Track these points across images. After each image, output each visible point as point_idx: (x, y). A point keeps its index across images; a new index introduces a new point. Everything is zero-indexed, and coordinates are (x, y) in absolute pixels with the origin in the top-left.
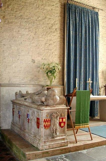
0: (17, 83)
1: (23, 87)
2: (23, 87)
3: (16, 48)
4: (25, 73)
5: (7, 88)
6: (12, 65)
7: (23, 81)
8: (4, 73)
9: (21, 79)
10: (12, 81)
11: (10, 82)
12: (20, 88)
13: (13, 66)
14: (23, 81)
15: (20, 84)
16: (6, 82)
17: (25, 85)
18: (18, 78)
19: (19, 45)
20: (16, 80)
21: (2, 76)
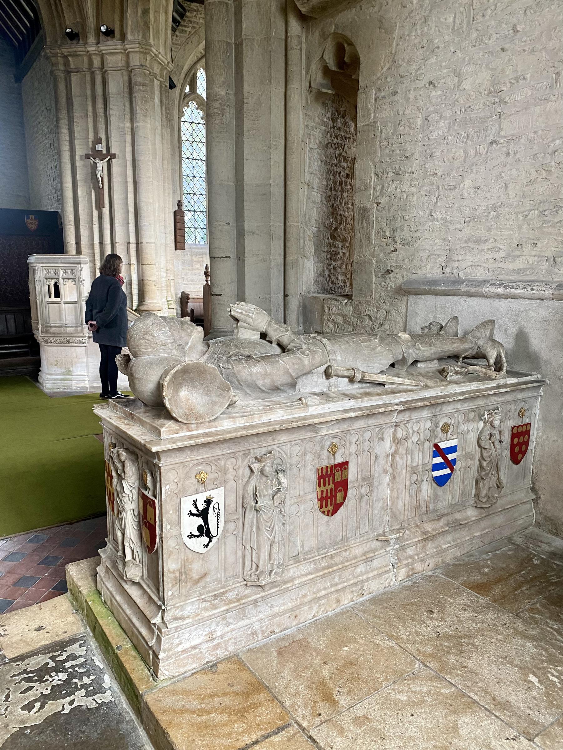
0: (480, 274)
1: (499, 296)
2: (499, 296)
3: (485, 76)
4: (526, 216)
5: (431, 300)
6: (463, 180)
7: (510, 266)
8: (426, 227)
9: (502, 254)
10: (456, 264)
11: (448, 270)
12: (488, 301)
13: (468, 183)
14: (510, 266)
15: (483, 283)
16: (430, 270)
17: (508, 289)
18: (485, 247)
19: (503, 50)
20: (472, 264)
21: (416, 245)
